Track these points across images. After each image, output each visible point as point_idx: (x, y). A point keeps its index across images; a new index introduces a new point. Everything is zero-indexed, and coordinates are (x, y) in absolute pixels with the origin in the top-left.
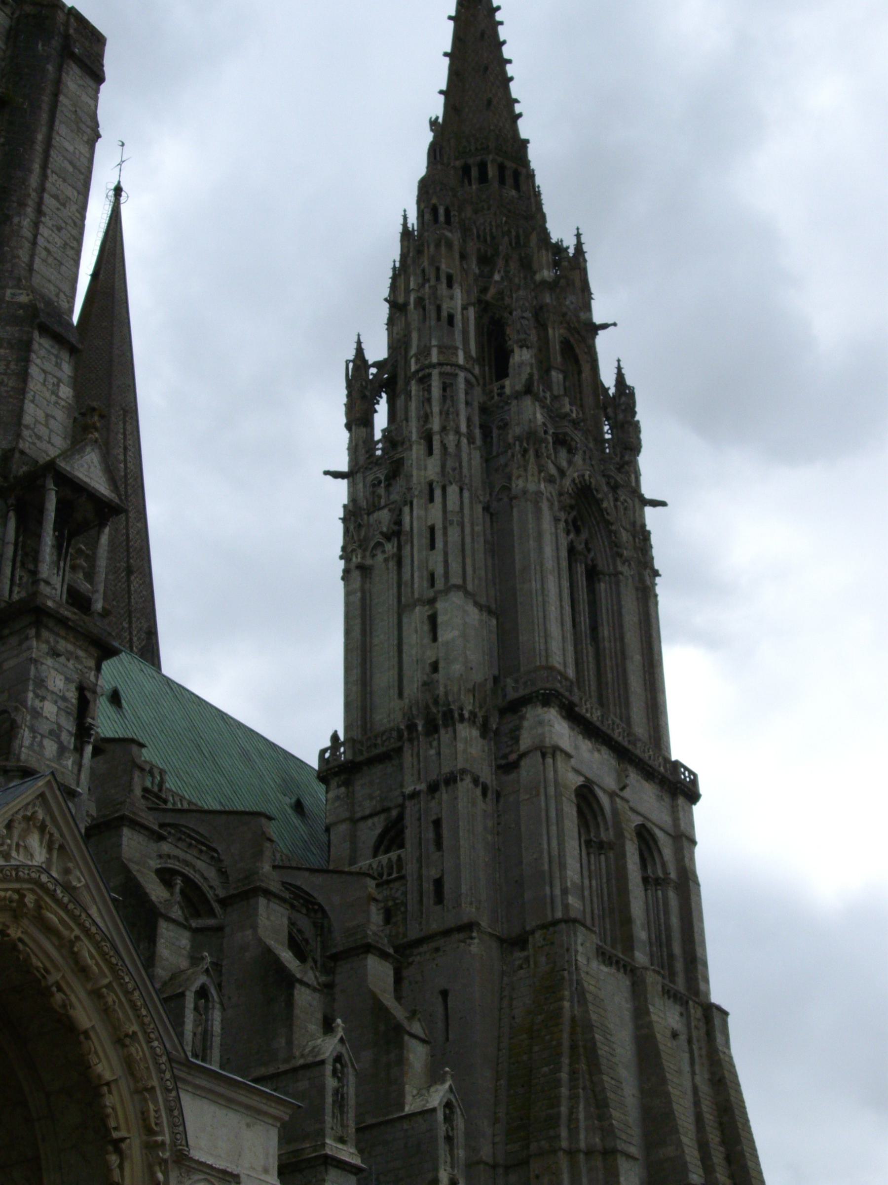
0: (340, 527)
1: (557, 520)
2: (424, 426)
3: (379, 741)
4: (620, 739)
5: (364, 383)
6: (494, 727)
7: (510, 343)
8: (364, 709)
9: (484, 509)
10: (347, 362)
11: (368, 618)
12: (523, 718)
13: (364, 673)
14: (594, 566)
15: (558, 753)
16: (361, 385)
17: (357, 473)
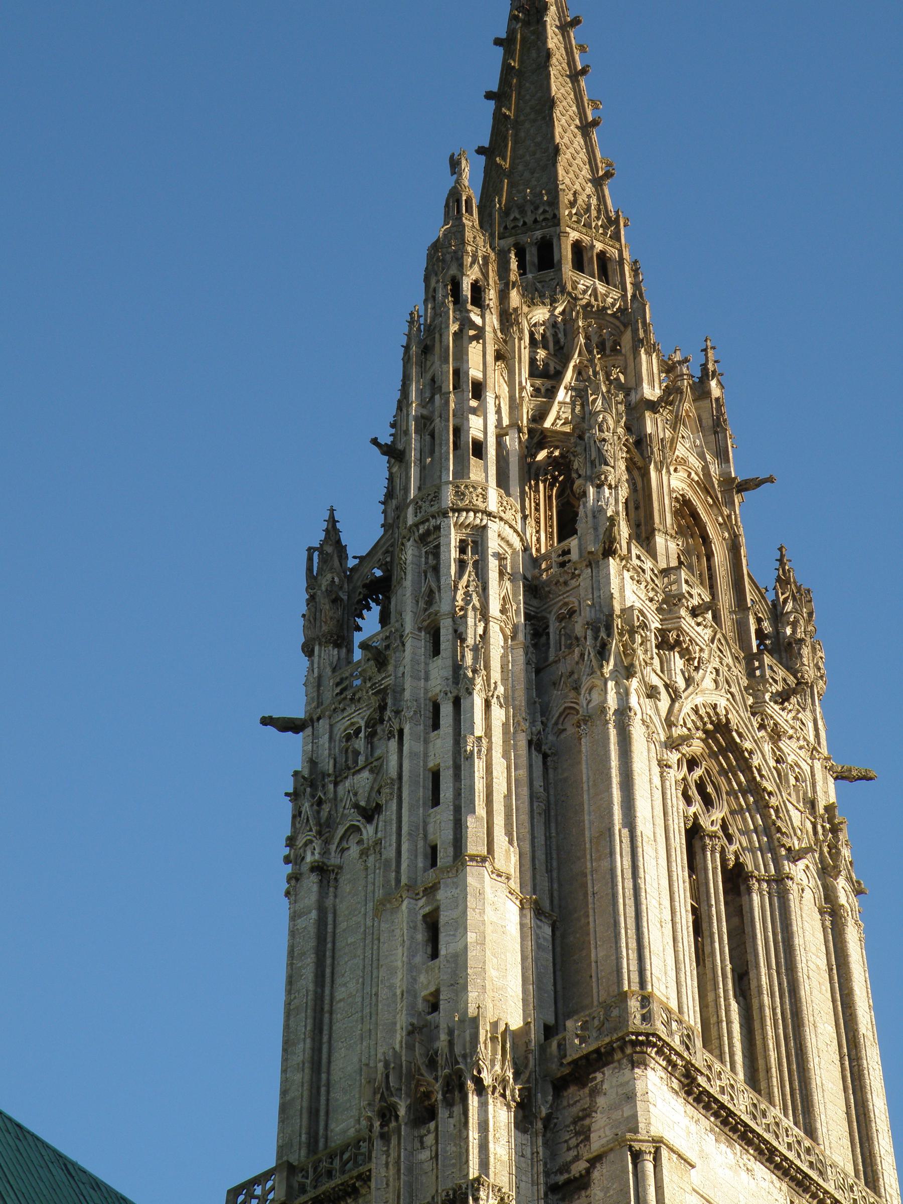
0: (287, 807)
1: (663, 765)
2: (426, 610)
3: (337, 1163)
4: (791, 1155)
5: (336, 580)
6: (544, 1112)
7: (578, 482)
8: (314, 1113)
9: (530, 743)
10: (311, 550)
11: (328, 954)
12: (595, 1092)
13: (317, 1050)
14: (739, 866)
15: (664, 1152)
16: (333, 581)
17: (319, 719)
